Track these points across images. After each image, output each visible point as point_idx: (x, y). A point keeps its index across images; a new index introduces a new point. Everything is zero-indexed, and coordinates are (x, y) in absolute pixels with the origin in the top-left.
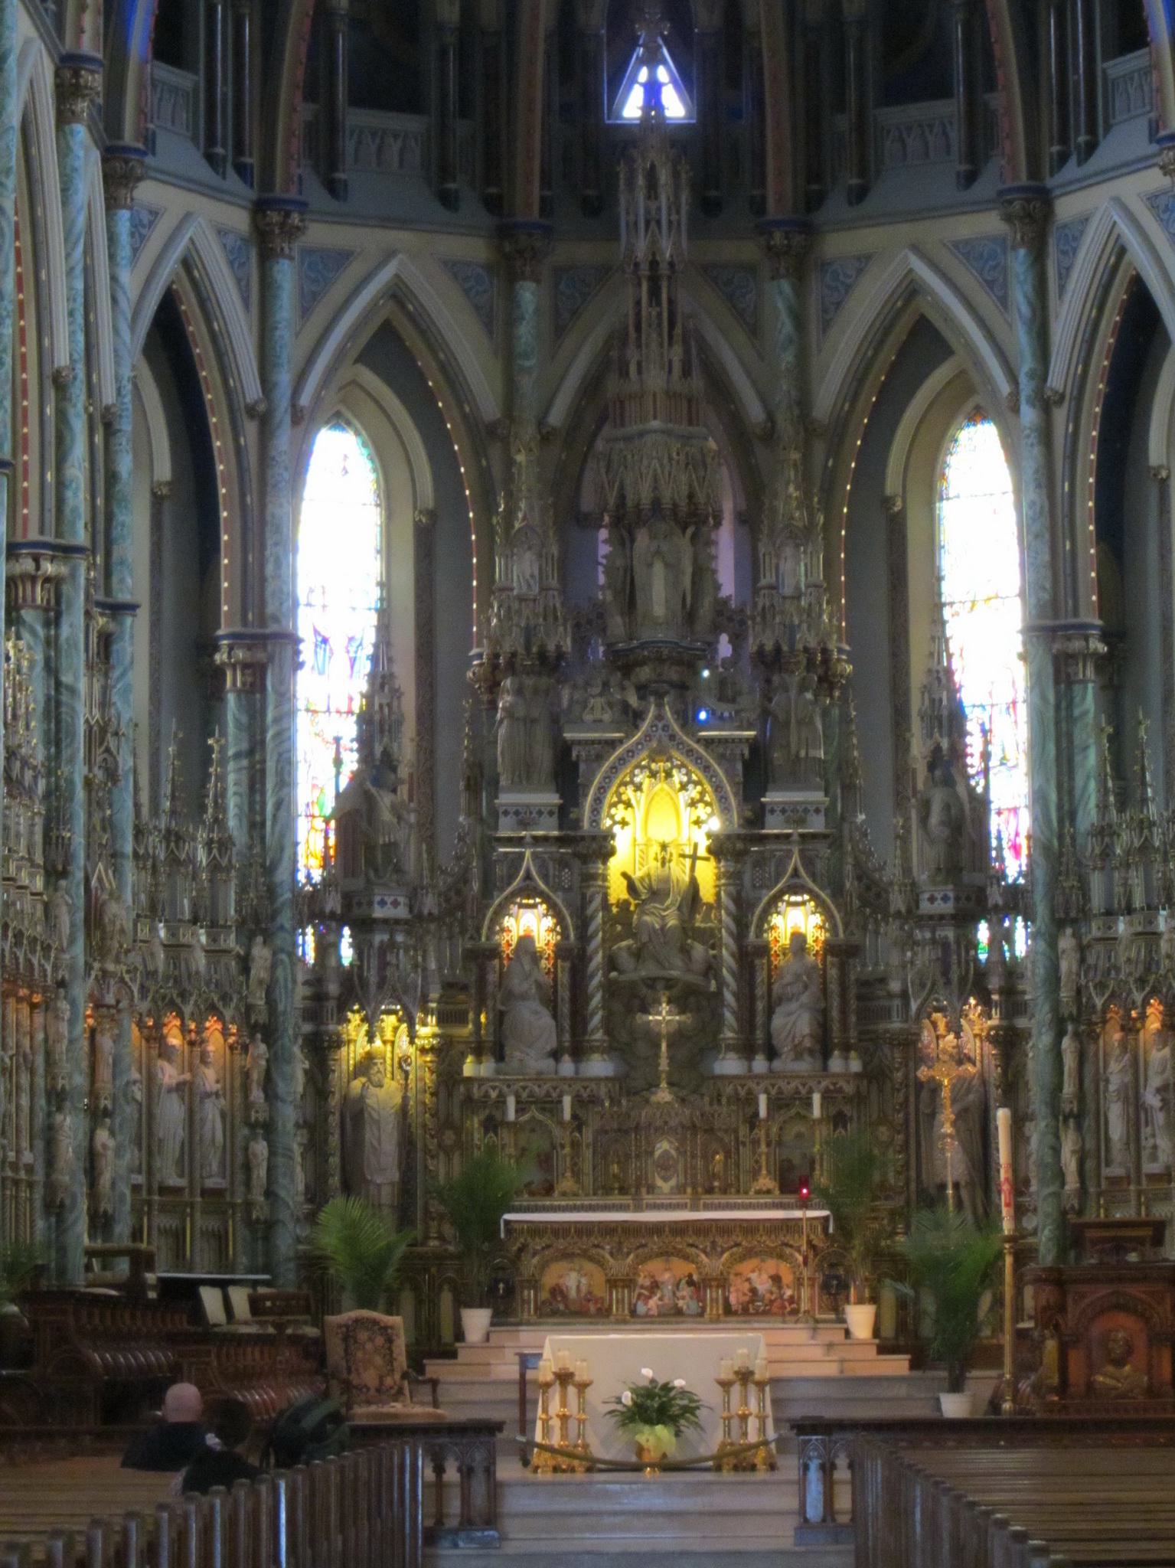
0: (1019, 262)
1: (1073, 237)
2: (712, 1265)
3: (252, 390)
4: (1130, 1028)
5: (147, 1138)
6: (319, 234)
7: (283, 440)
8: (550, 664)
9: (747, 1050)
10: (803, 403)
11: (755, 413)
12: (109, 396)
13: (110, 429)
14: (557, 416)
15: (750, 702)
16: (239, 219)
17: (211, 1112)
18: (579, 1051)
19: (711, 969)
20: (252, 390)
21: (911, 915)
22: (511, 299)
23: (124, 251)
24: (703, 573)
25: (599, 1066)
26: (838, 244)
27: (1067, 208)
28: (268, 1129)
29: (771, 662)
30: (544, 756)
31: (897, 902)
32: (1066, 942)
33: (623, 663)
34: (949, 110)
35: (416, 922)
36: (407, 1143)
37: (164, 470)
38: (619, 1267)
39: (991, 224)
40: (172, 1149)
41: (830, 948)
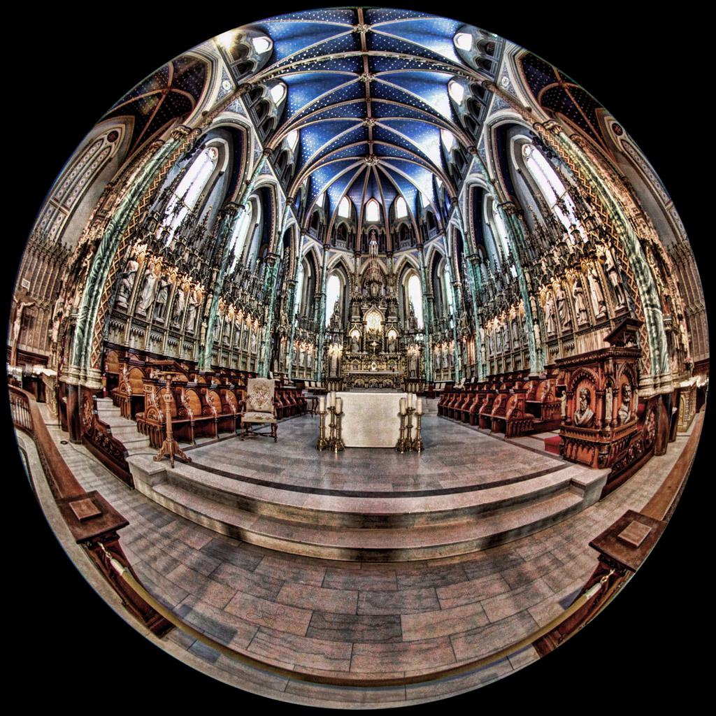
0: (420, 253)
1: (427, 249)
2: (381, 380)
3: (321, 265)
4: (441, 347)
5: (297, 358)
6: (331, 250)
7: (325, 271)
8: (360, 300)
9: (385, 351)
10: (392, 272)
11: (386, 273)
12: (297, 255)
13: (297, 259)
14: (361, 273)
15: (386, 305)
16: (322, 246)
17: (309, 357)
18: (362, 351)
19: (381, 340)
20: (321, 265)
21: (409, 334)
22: (356, 260)
23: (302, 242)
24: (380, 289)
25: (365, 353)
26: (395, 255)
27: (425, 247)
28: (317, 359)
29: (388, 301)
30: (358, 312)
31: (406, 332)
32: (430, 336)
33: (369, 300)
34: (409, 241)
35: (340, 333)
36: (338, 363)
37: (310, 275)
38: (367, 380)
39: (416, 250)
40: (302, 361)
41: (397, 338)
